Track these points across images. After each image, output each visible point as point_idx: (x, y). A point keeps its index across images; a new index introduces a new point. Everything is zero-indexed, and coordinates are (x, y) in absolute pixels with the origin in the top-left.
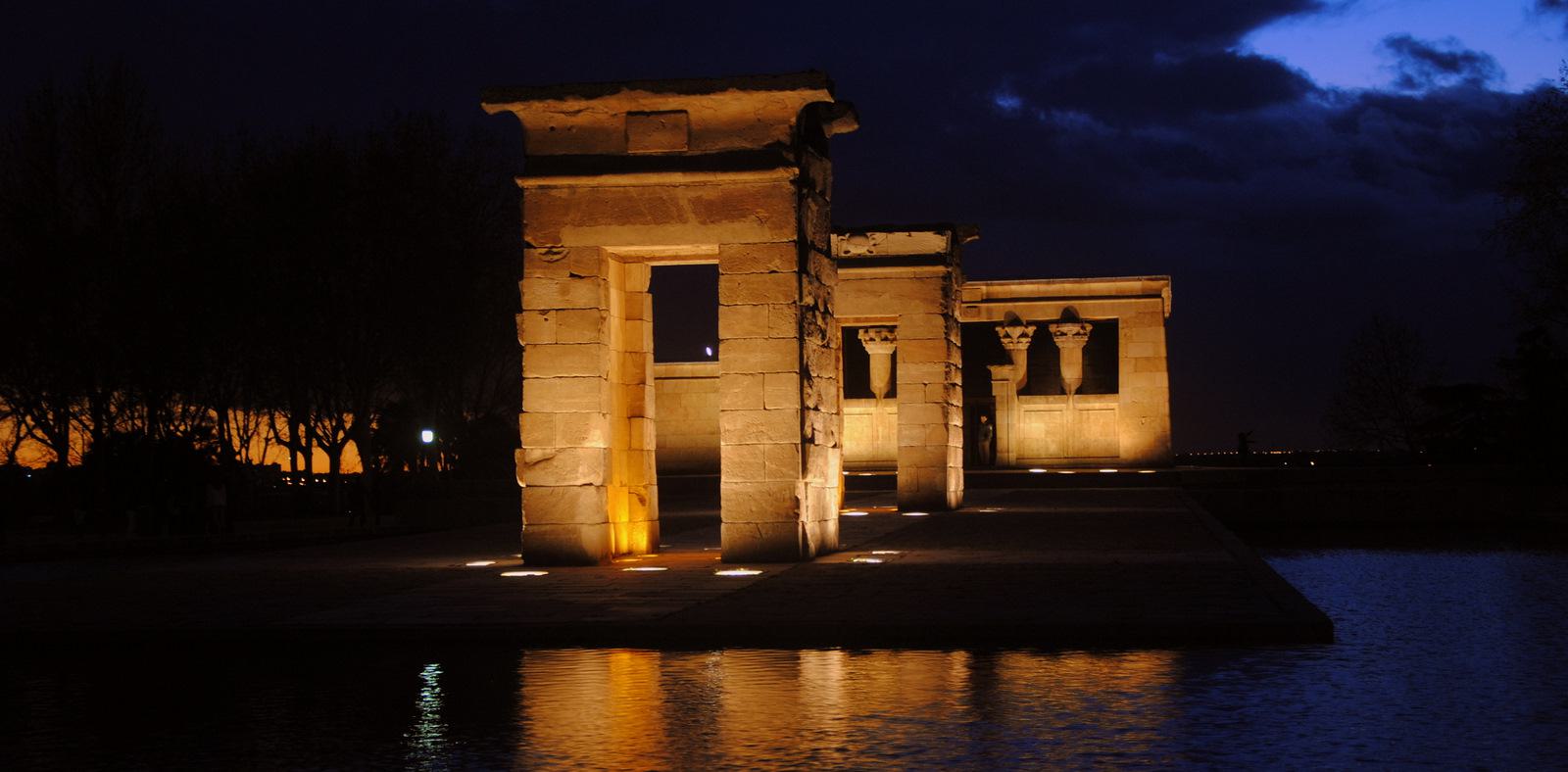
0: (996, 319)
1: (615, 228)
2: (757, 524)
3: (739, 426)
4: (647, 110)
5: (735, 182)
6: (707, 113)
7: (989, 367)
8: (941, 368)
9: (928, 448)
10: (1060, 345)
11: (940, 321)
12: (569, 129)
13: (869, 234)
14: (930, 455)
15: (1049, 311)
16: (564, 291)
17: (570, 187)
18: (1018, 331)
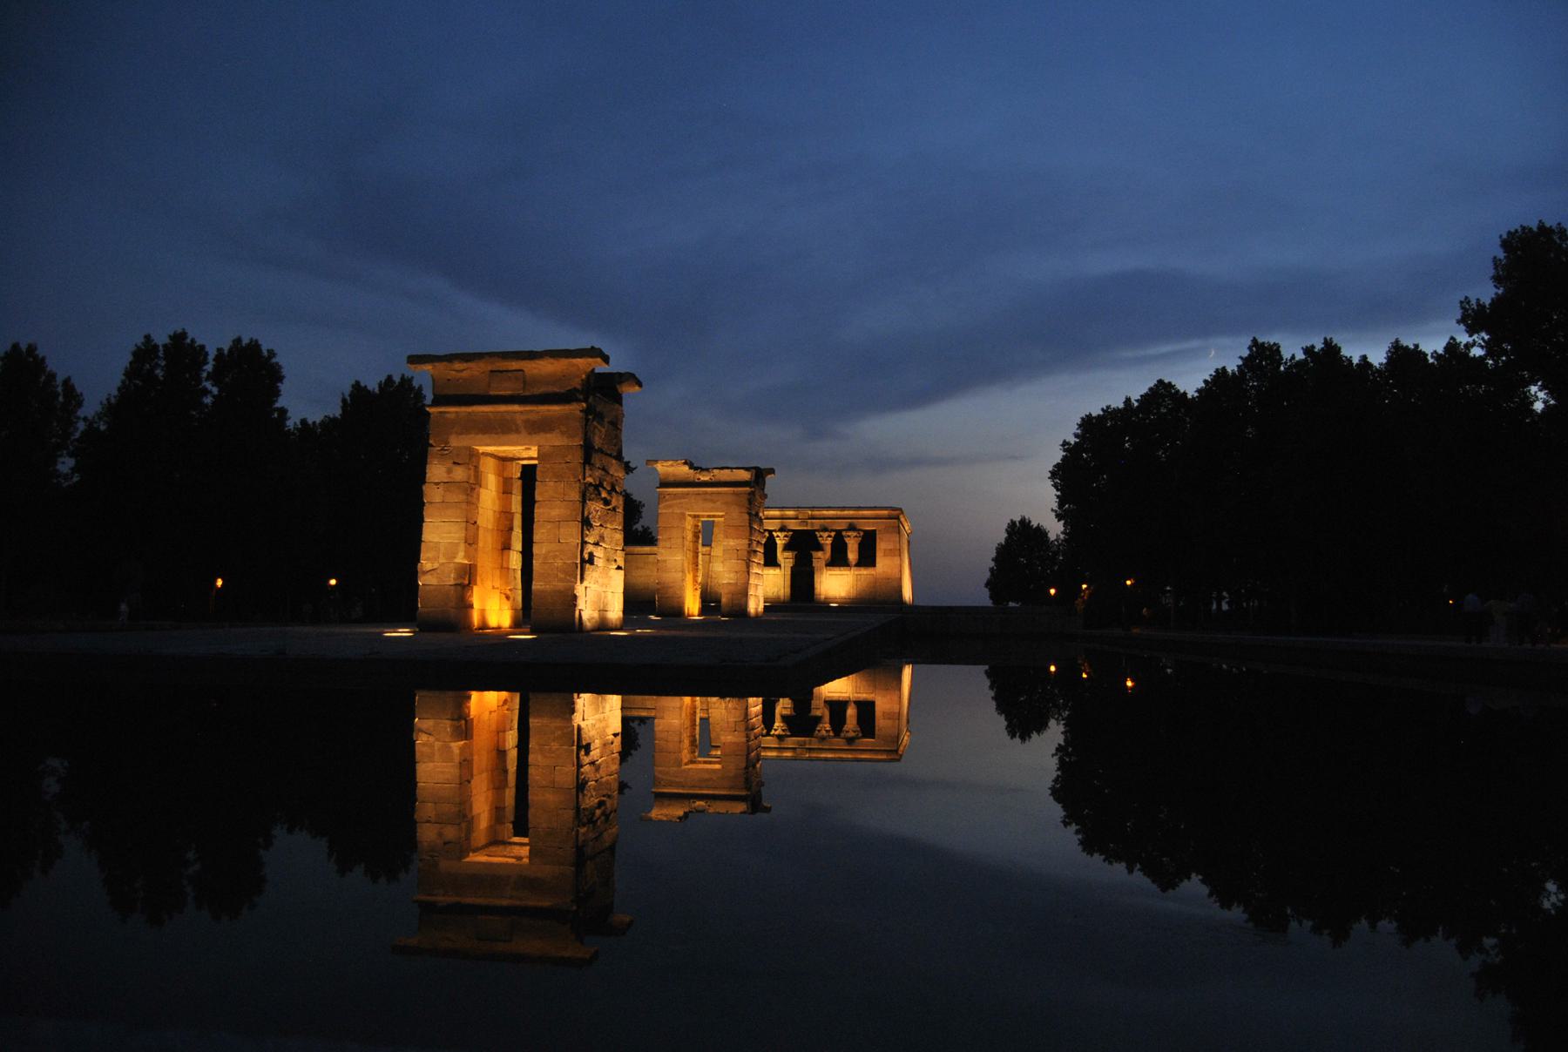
1: (480, 436)
3: (544, 552)
4: (501, 369)
5: (549, 411)
6: (535, 371)
8: (747, 542)
11: (747, 517)
12: (458, 380)
15: (841, 525)
16: (449, 471)
17: (457, 412)
18: (826, 534)
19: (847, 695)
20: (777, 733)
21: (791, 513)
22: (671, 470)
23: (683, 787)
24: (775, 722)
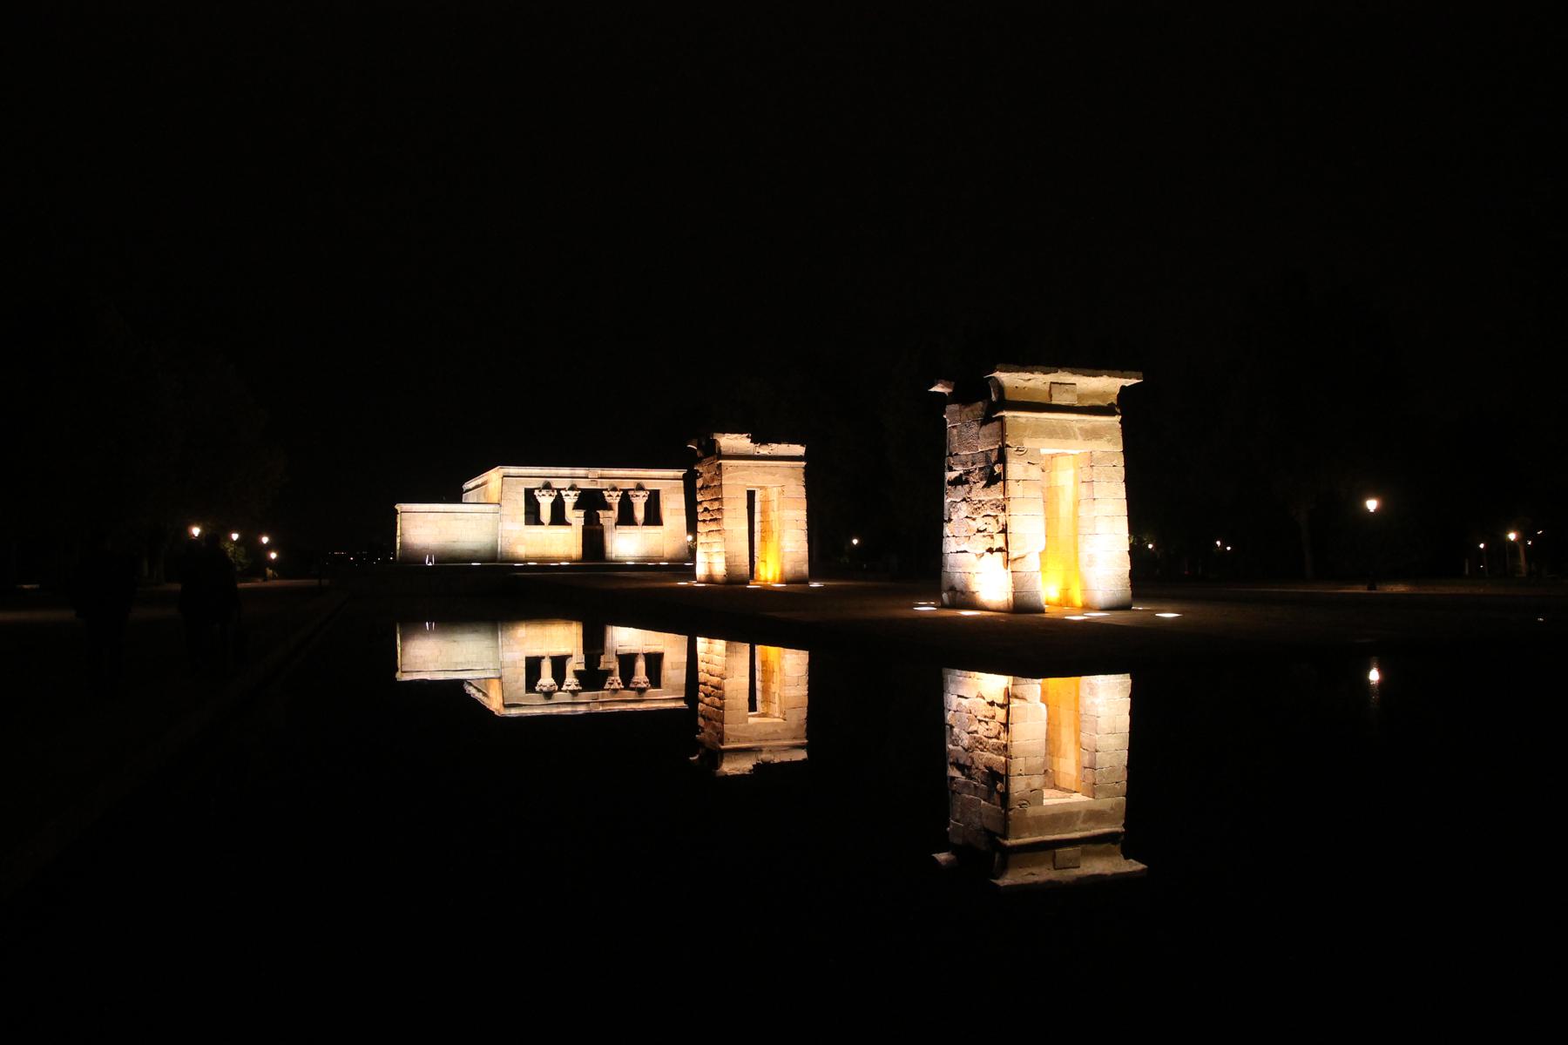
0: (604, 487)
1: (1046, 440)
5: (1097, 421)
7: (601, 512)
10: (634, 502)
15: (630, 484)
16: (1026, 471)
17: (1027, 417)
18: (617, 493)
19: (637, 648)
20: (570, 688)
21: (580, 471)
23: (750, 741)
24: (565, 678)
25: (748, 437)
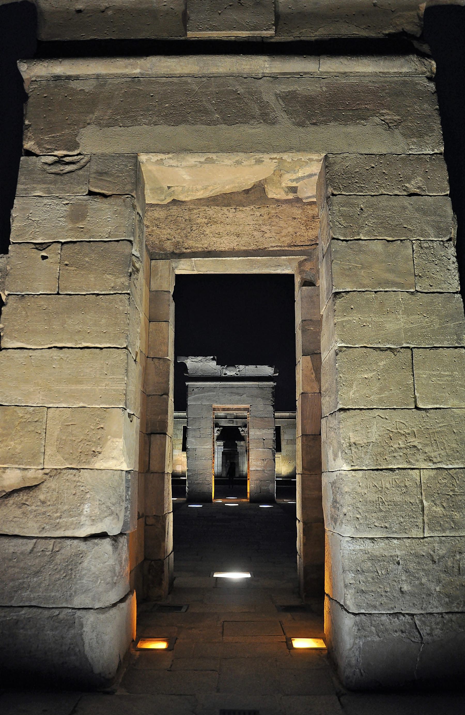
2: (412, 615)
7: (236, 442)
9: (265, 471)
13: (236, 366)
14: (266, 475)
22: (200, 365)
25: (213, 359)
